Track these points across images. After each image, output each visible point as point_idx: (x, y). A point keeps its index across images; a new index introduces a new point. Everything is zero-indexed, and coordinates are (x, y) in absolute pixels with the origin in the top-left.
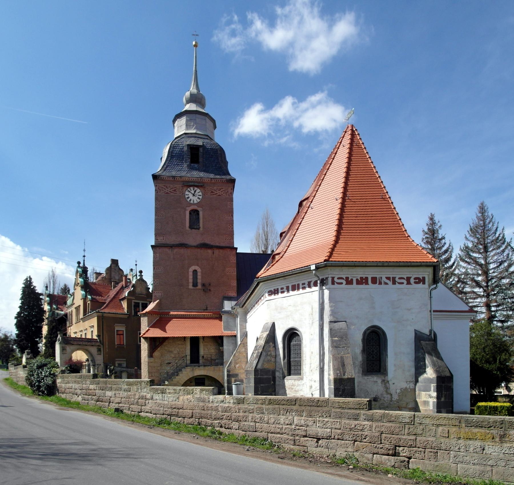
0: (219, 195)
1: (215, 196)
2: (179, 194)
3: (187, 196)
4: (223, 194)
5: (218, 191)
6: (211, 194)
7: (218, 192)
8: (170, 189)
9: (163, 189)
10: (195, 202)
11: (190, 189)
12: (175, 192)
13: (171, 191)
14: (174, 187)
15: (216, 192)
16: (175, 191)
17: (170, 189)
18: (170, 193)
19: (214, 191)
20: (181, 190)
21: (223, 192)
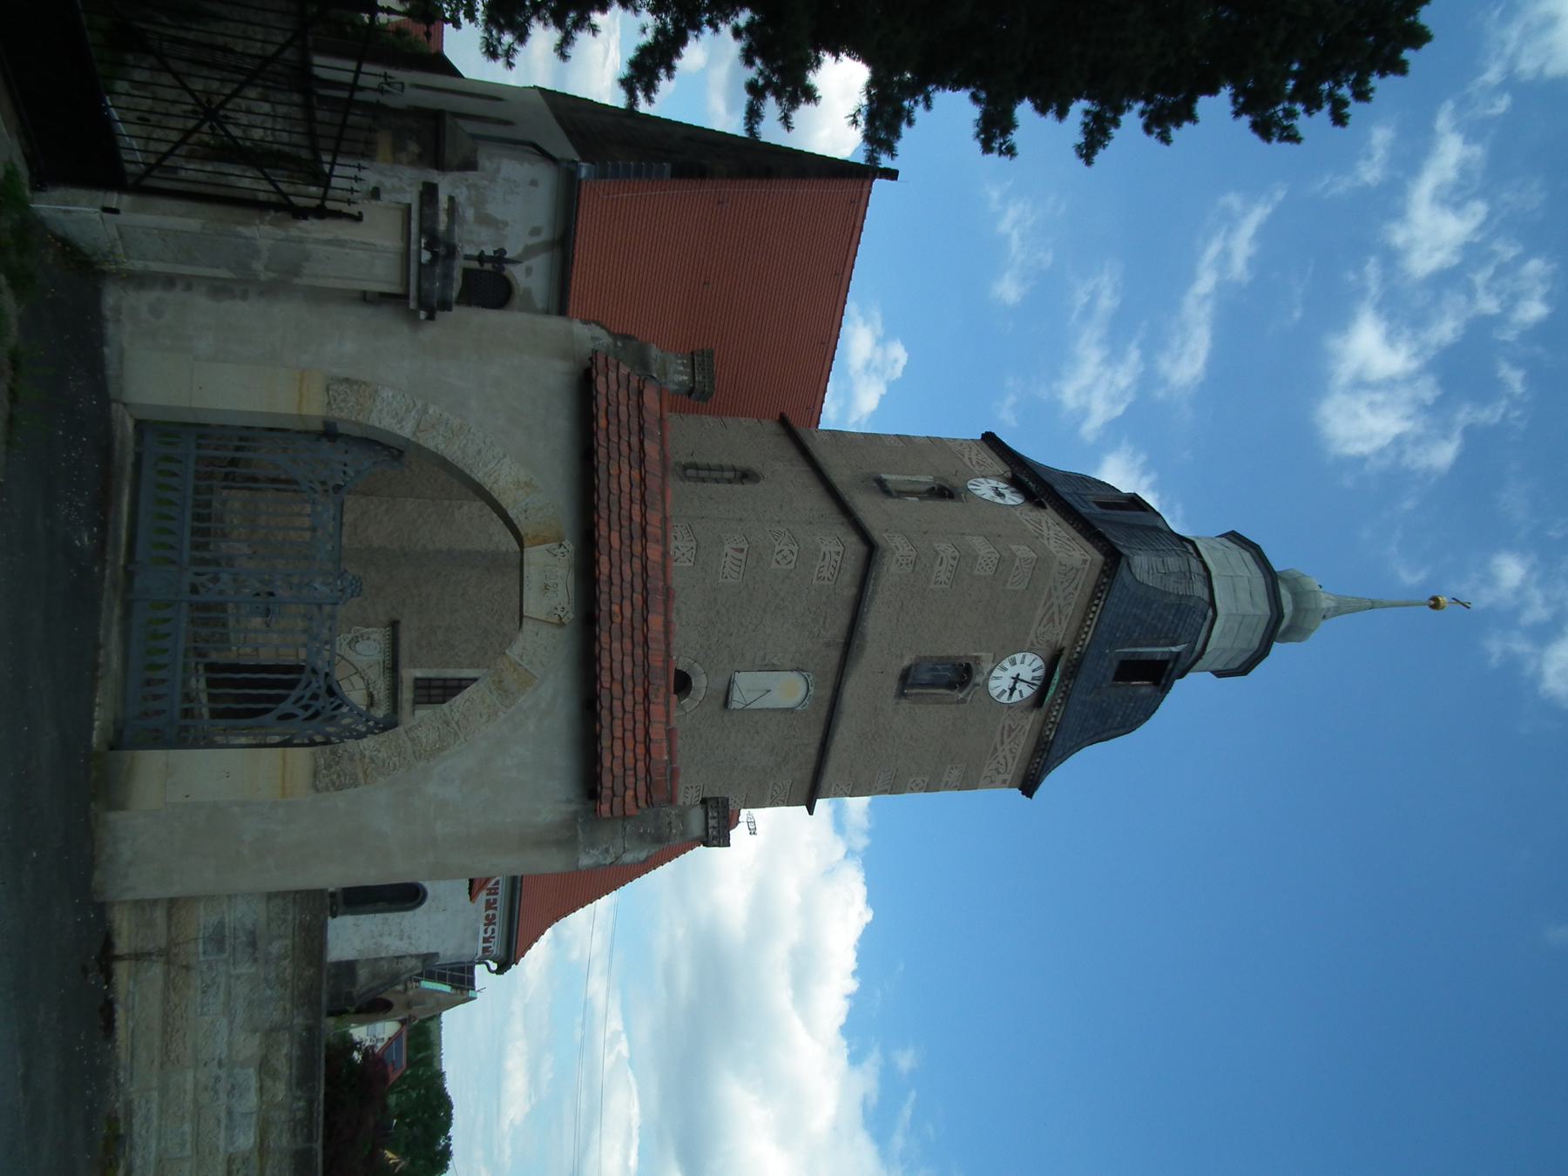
0: (996, 749)
1: (998, 738)
2: (1032, 632)
3: (1018, 657)
4: (997, 760)
5: (1009, 747)
6: (1007, 728)
7: (1007, 747)
8: (1059, 606)
9: (1066, 584)
10: (992, 684)
11: (1039, 668)
12: (1045, 622)
13: (1055, 609)
14: (1063, 618)
15: (1006, 741)
16: (1052, 620)
17: (1059, 606)
18: (1049, 603)
19: (1013, 735)
20: (1047, 638)
21: (1003, 761)
